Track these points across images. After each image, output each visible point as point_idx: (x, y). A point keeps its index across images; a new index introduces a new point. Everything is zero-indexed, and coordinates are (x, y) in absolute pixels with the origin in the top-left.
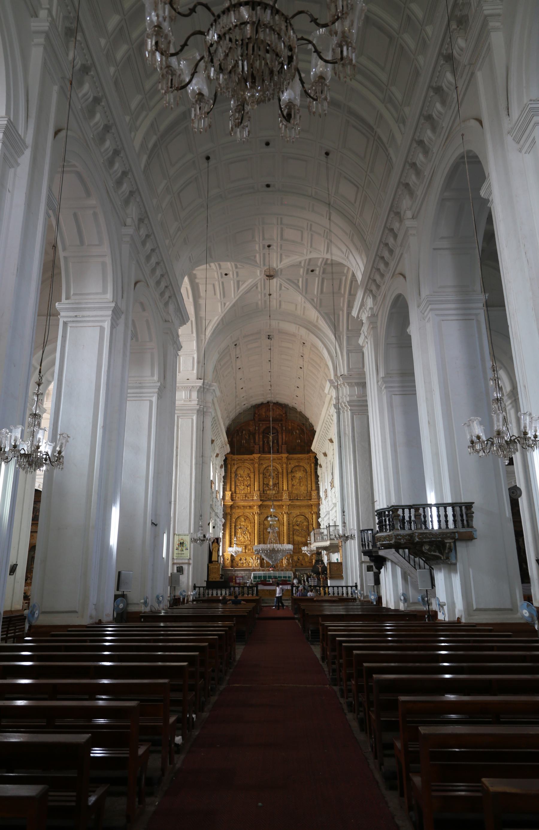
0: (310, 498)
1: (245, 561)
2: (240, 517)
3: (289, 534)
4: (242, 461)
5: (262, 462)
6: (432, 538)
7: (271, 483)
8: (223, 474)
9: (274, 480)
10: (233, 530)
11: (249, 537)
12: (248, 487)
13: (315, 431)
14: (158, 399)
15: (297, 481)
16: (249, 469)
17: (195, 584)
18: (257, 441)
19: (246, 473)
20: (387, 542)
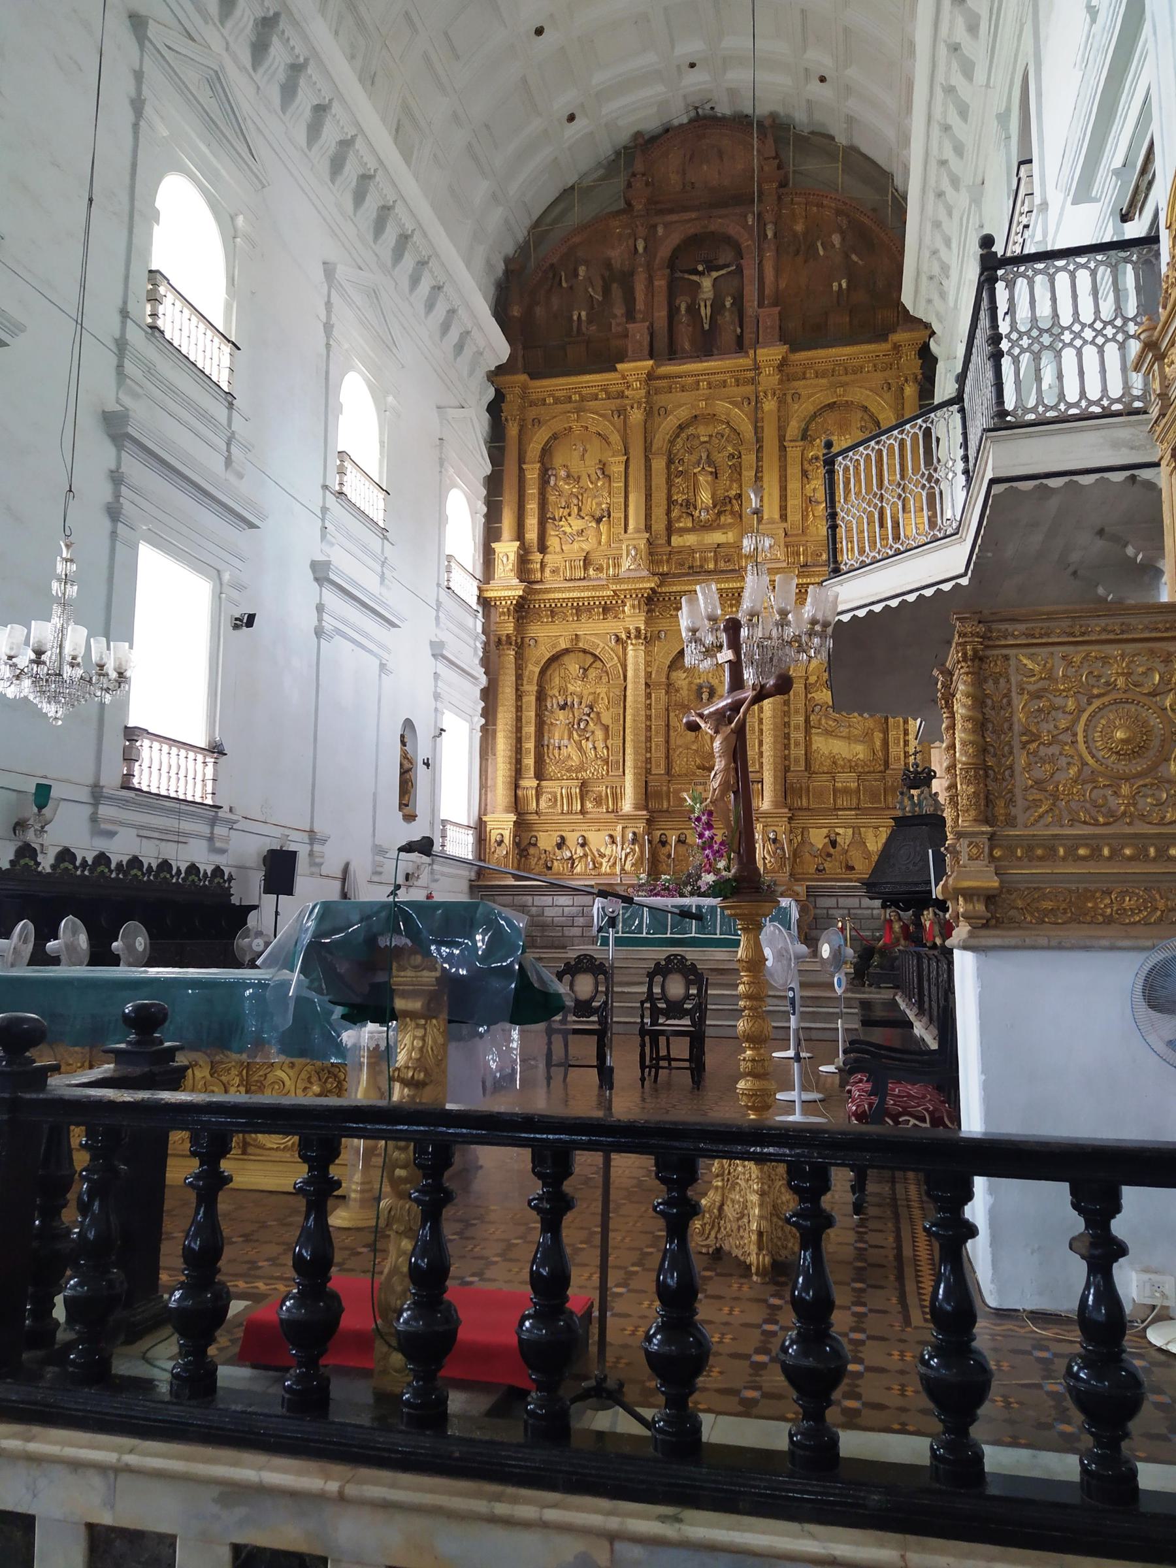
1: (580, 852)
2: (566, 659)
3: (787, 725)
4: (572, 405)
5: (661, 400)
7: (705, 497)
11: (600, 745)
12: (599, 521)
18: (640, 305)
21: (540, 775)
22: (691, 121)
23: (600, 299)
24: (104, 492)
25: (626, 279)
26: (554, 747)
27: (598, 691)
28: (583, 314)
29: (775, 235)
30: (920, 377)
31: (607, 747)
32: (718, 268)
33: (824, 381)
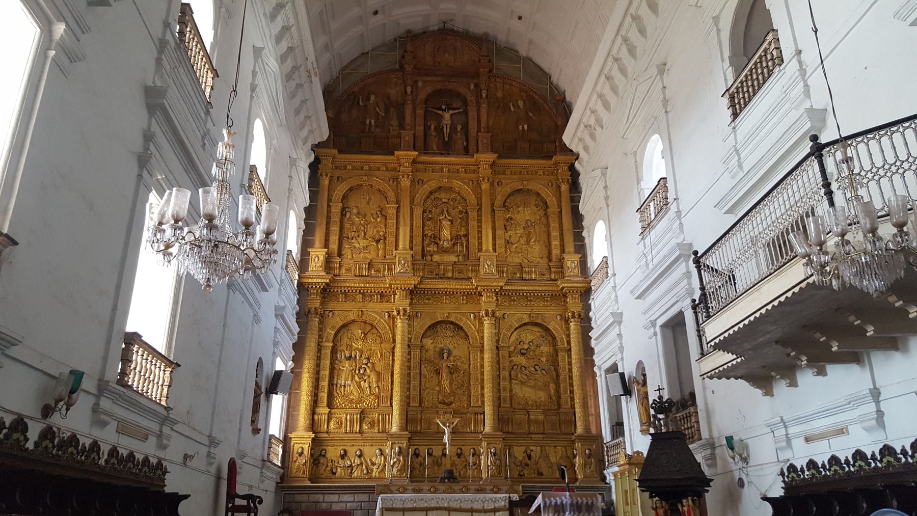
1: (357, 461)
2: (352, 327)
3: (499, 376)
5: (420, 175)
10: (327, 362)
12: (378, 242)
15: (520, 231)
21: (330, 405)
22: (438, 30)
23: (383, 114)
24: (137, 143)
25: (400, 107)
26: (341, 386)
28: (373, 121)
29: (487, 96)
30: (570, 181)
31: (378, 386)
32: (453, 109)
33: (516, 177)
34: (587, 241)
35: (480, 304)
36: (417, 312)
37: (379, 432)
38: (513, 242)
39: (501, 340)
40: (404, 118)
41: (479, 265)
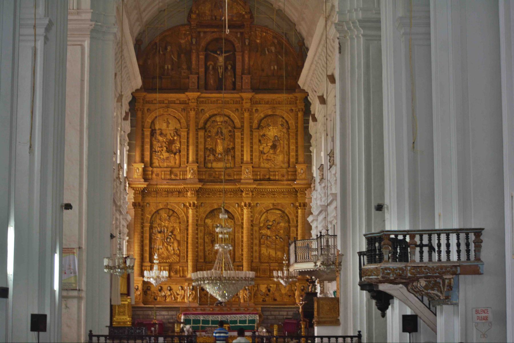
0: (293, 177)
1: (169, 293)
3: (252, 243)
4: (164, 105)
6: (427, 273)
7: (220, 149)
8: (128, 129)
9: (226, 142)
11: (177, 248)
13: (308, 49)
14: (45, 43)
16: (179, 120)
17: (91, 331)
18: (194, 66)
19: (171, 127)
20: (374, 277)
25: (188, 53)
27: (175, 226)
28: (170, 66)
30: (304, 110)
31: (179, 250)
34: (312, 154)
35: (242, 197)
36: (202, 203)
37: (180, 277)
38: (265, 152)
39: (254, 220)
40: (191, 63)
41: (241, 171)
